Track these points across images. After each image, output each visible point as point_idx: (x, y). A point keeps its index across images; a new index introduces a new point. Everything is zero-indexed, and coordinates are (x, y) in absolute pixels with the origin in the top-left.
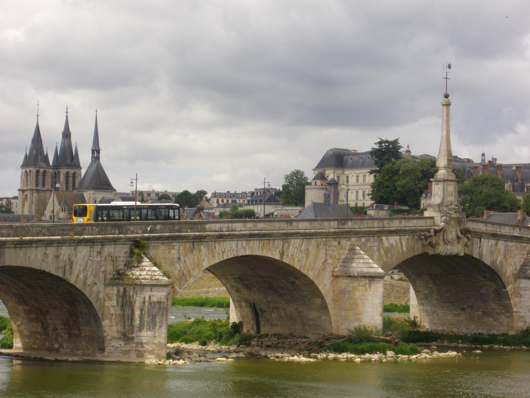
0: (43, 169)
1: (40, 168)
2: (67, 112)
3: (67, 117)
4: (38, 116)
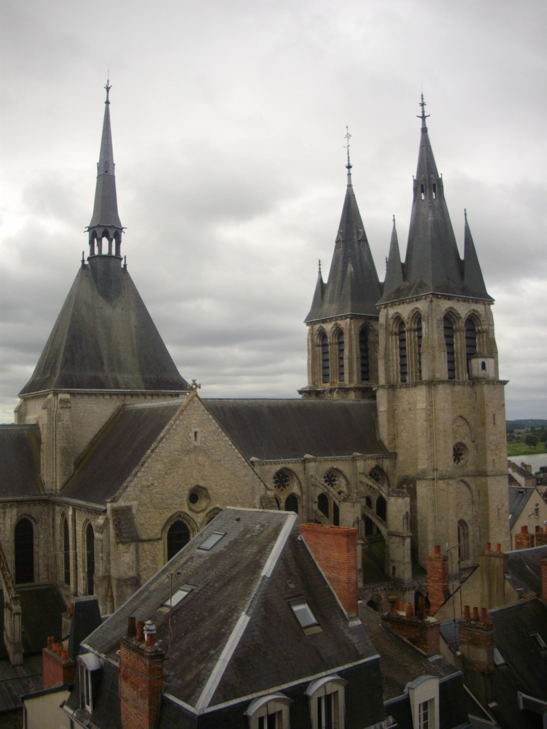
0: (333, 323)
1: (324, 321)
2: (423, 117)
3: (424, 130)
4: (349, 167)
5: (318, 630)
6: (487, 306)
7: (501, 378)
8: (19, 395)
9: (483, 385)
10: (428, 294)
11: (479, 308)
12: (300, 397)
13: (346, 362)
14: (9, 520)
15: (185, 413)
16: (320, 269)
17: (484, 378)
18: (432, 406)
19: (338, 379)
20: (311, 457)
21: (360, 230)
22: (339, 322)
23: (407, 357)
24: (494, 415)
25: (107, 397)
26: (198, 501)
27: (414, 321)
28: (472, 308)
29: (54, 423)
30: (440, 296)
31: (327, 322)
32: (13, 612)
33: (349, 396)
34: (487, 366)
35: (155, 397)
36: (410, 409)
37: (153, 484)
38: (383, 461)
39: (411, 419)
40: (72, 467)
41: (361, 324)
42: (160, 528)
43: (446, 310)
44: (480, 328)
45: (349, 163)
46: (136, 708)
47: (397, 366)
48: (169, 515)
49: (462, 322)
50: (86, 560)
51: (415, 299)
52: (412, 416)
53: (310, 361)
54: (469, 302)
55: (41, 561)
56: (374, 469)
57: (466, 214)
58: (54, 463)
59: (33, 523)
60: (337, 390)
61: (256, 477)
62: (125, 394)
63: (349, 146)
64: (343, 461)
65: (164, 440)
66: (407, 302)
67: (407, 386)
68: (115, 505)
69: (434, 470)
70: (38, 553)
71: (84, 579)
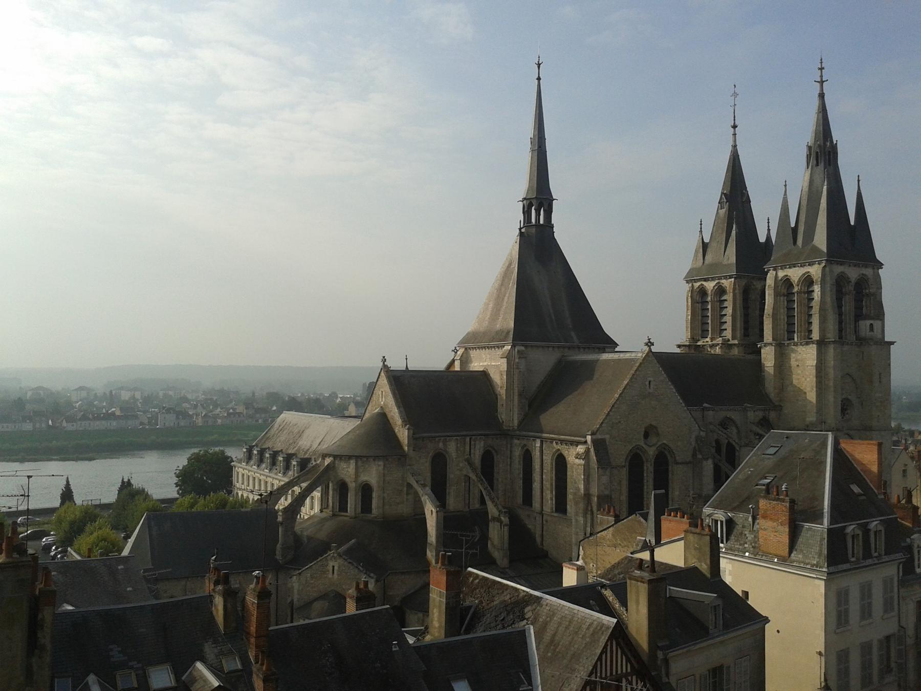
1: (706, 280)
3: (822, 96)
4: (735, 127)
5: (864, 497)
6: (876, 270)
7: (886, 340)
8: (458, 344)
9: (871, 345)
10: (823, 260)
11: (869, 272)
12: (678, 350)
13: (728, 319)
14: (478, 451)
15: (642, 365)
16: (701, 228)
17: (872, 339)
18: (822, 364)
19: (718, 334)
20: (709, 406)
21: (744, 191)
22: (723, 281)
23: (796, 317)
24: (880, 374)
25: (551, 349)
26: (649, 437)
27: (803, 284)
28: (861, 272)
29: (512, 370)
30: (833, 262)
31: (709, 280)
32: (504, 523)
33: (732, 351)
34: (875, 327)
35: (586, 350)
36: (798, 366)
37: (620, 422)
38: (769, 413)
39: (798, 374)
40: (527, 409)
41: (744, 283)
42: (624, 457)
43: (838, 274)
44: (867, 291)
45: (734, 123)
46: (776, 532)
47: (784, 325)
48: (631, 448)
49: (852, 286)
50: (554, 484)
51: (807, 264)
52: (799, 372)
53: (690, 317)
54: (859, 267)
55: (500, 486)
56: (762, 419)
57: (859, 181)
58: (512, 404)
59: (495, 454)
60: (720, 345)
61: (692, 419)
62: (564, 347)
63: (735, 105)
64: (735, 410)
65: (628, 387)
66: (798, 266)
67: (796, 344)
68: (594, 437)
69: (822, 422)
70: (498, 480)
71: (552, 499)
